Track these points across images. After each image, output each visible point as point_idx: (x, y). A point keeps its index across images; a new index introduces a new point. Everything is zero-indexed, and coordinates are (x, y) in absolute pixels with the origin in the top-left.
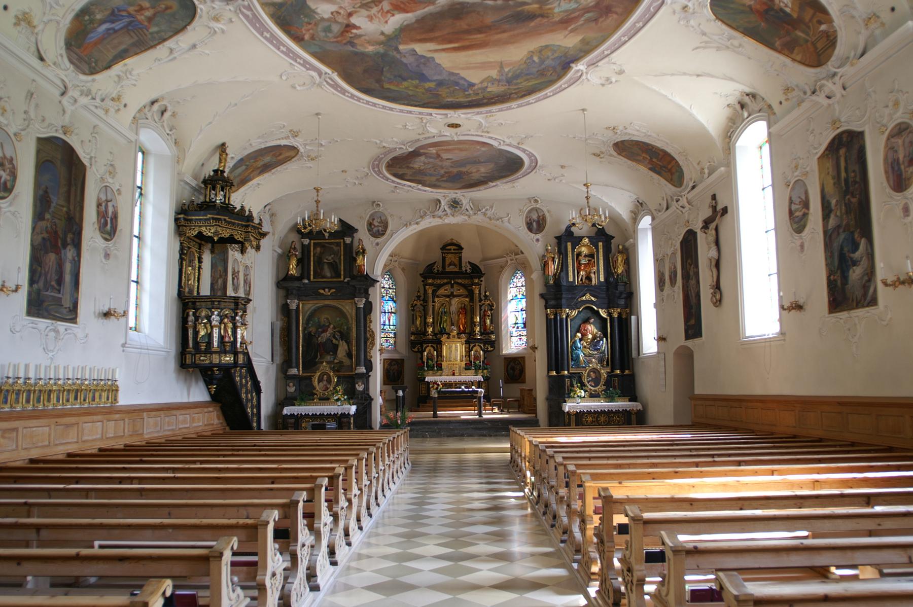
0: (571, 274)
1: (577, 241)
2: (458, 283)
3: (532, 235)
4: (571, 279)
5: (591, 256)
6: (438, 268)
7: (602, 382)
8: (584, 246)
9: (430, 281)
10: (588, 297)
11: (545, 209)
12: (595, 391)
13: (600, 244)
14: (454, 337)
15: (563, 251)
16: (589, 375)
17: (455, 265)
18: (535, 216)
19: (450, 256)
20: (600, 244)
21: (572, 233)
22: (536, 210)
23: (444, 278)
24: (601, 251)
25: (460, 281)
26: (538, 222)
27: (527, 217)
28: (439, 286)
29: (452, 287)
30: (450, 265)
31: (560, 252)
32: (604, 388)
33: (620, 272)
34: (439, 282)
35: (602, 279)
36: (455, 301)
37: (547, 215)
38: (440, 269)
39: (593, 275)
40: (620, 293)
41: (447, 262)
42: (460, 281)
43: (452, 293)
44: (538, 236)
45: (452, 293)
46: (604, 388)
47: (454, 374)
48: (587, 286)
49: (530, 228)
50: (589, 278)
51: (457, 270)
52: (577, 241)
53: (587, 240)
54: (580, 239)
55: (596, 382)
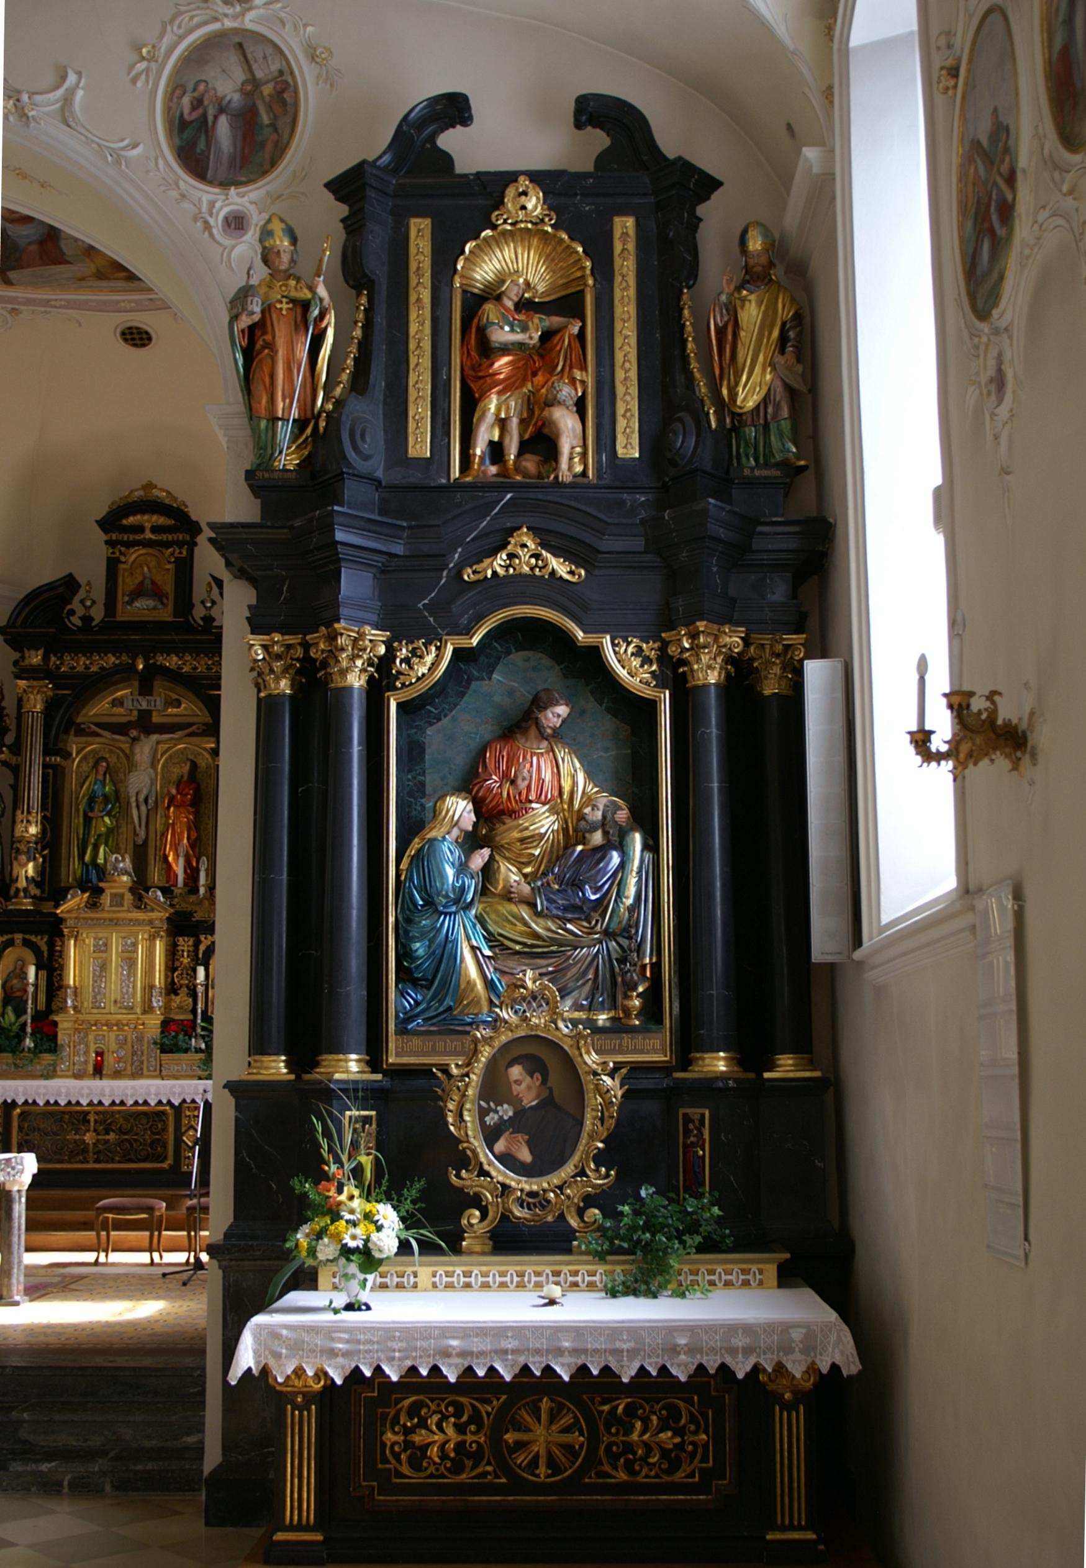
0: (420, 411)
1: (470, 206)
2: (165, 672)
3: (204, 194)
4: (420, 445)
5: (567, 304)
6: (88, 604)
7: (592, 1136)
8: (517, 235)
9: (35, 658)
10: (526, 555)
11: (292, 43)
12: (535, 1199)
13: (625, 226)
14: (118, 899)
15: (377, 266)
16: (493, 1088)
17: (157, 593)
18: (227, 83)
19: (134, 554)
20: (625, 226)
21: (447, 160)
22: (240, 43)
23: (103, 649)
24: (626, 266)
25: (172, 661)
26: (246, 120)
27: (176, 88)
28: (89, 686)
29: (146, 689)
30: (137, 593)
31: (354, 272)
32: (599, 1179)
33: (748, 397)
34: (80, 663)
35: (629, 447)
36: (144, 749)
37: (307, 77)
38: (98, 614)
39: (567, 423)
40: (754, 528)
41: (127, 582)
42: (172, 661)
43: (145, 716)
44: (245, 199)
45: (145, 715)
46: (599, 1179)
47: (98, 1071)
48: (528, 492)
49: (194, 156)
50: (542, 442)
51: (166, 614)
52: (470, 206)
53: (534, 203)
54: (491, 188)
55: (548, 1133)
